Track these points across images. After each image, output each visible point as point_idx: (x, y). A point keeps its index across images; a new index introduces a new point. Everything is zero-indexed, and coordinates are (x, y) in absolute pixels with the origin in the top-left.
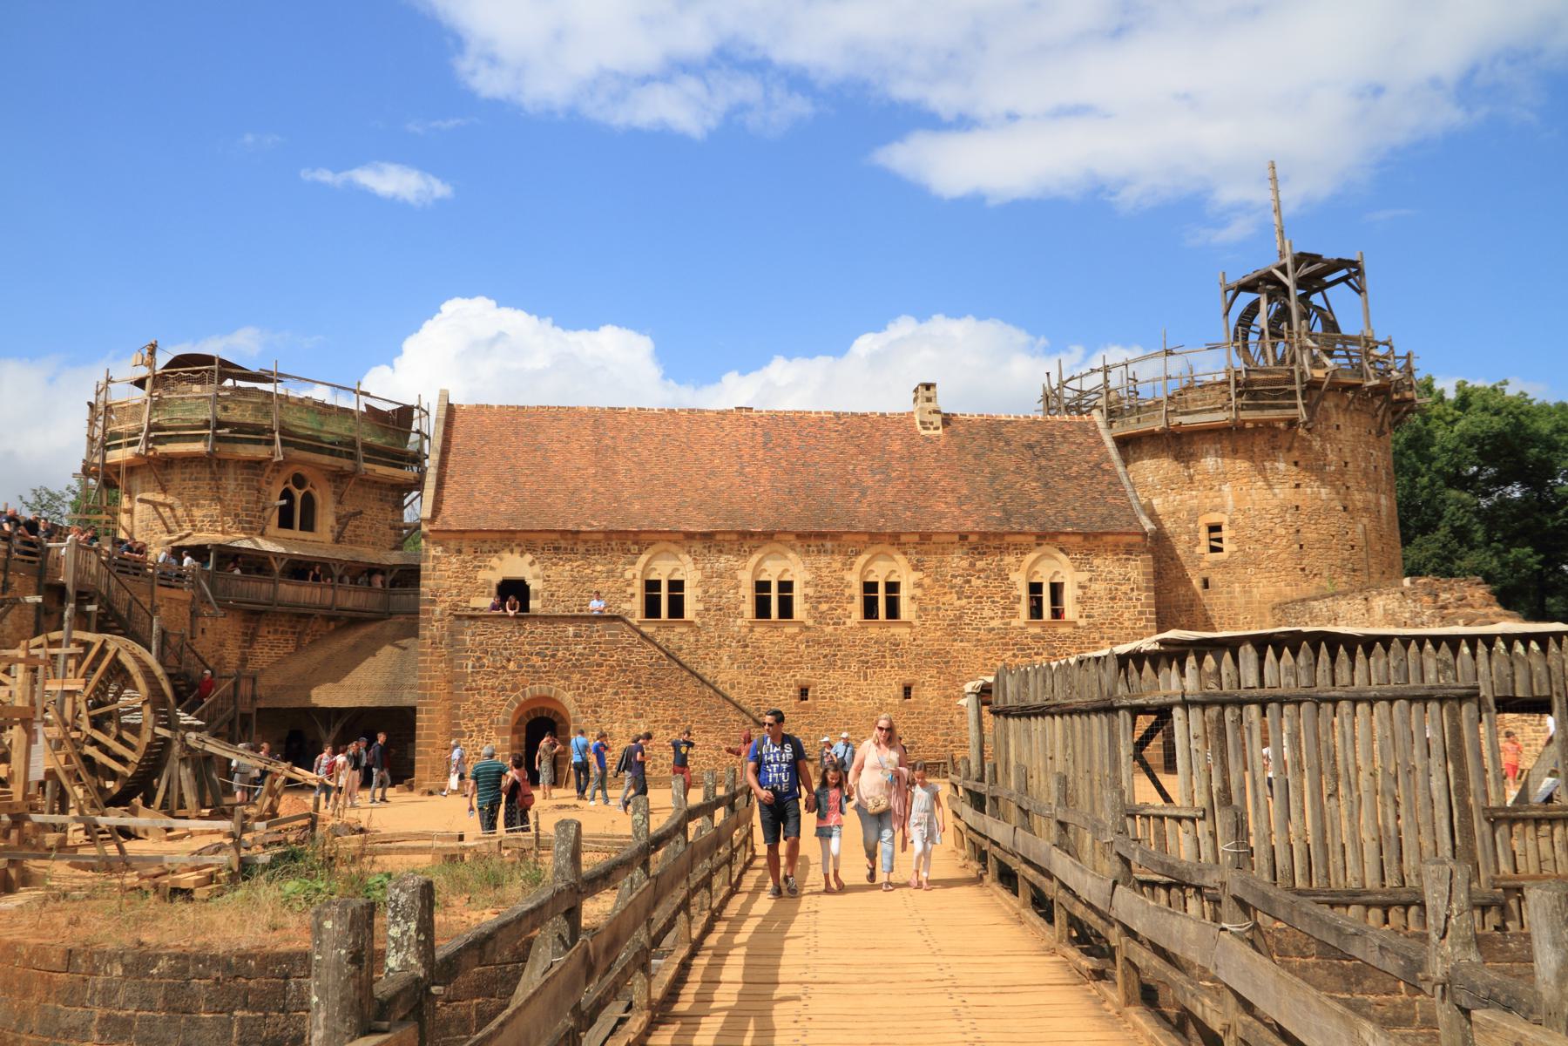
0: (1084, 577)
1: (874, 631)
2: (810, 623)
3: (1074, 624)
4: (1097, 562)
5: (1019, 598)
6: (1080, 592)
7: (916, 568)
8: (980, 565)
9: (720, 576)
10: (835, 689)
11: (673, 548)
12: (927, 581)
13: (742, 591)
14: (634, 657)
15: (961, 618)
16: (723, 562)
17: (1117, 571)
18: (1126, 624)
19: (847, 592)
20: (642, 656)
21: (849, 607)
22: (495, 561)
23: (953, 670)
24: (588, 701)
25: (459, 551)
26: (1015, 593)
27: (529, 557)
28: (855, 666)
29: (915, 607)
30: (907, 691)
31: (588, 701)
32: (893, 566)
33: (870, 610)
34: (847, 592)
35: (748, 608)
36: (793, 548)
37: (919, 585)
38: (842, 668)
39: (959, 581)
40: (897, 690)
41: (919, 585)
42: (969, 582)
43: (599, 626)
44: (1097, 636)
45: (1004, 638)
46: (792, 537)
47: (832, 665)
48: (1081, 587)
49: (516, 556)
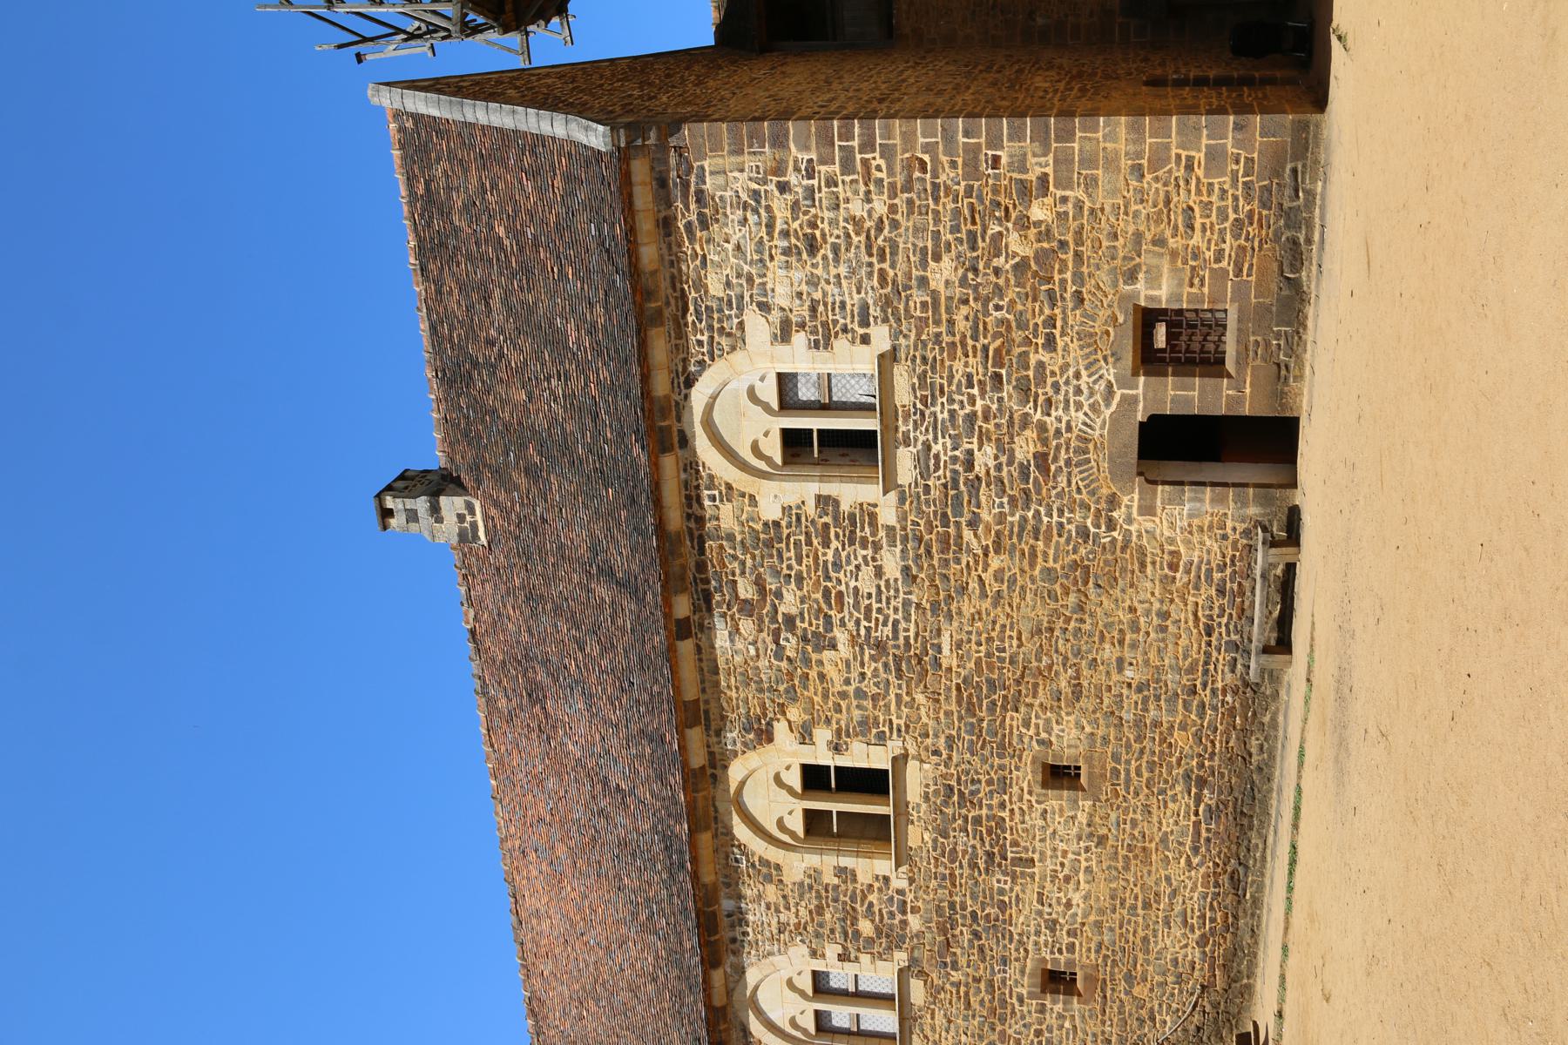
0: (758, 327)
1: (917, 836)
2: (901, 957)
3: (887, 360)
4: (715, 287)
5: (823, 501)
6: (800, 339)
7: (766, 736)
8: (746, 590)
10: (1052, 925)
12: (794, 713)
15: (880, 646)
17: (734, 230)
18: (880, 207)
19: (830, 878)
21: (864, 878)
23: (1009, 675)
26: (811, 509)
28: (997, 880)
30: (1059, 775)
33: (874, 832)
34: (830, 878)
37: (805, 736)
38: (1003, 906)
39: (791, 645)
41: (805, 736)
42: (790, 621)
44: (918, 296)
45: (934, 539)
46: (717, 976)
47: (999, 927)
48: (784, 334)
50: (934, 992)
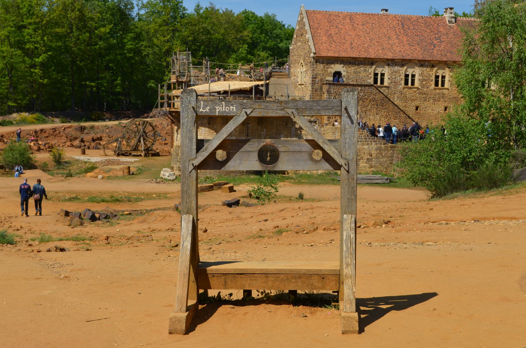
1: (438, 91)
2: (420, 87)
9: (396, 72)
10: (426, 108)
11: (383, 63)
13: (401, 77)
14: (376, 97)
16: (396, 68)
20: (379, 96)
22: (333, 66)
24: (364, 109)
25: (323, 63)
27: (342, 65)
29: (450, 84)
30: (446, 109)
31: (364, 109)
32: (444, 71)
35: (403, 82)
36: (416, 64)
40: (443, 108)
41: (452, 77)
43: (367, 88)
46: (416, 61)
47: (425, 100)
49: (339, 65)
50: (415, 92)
